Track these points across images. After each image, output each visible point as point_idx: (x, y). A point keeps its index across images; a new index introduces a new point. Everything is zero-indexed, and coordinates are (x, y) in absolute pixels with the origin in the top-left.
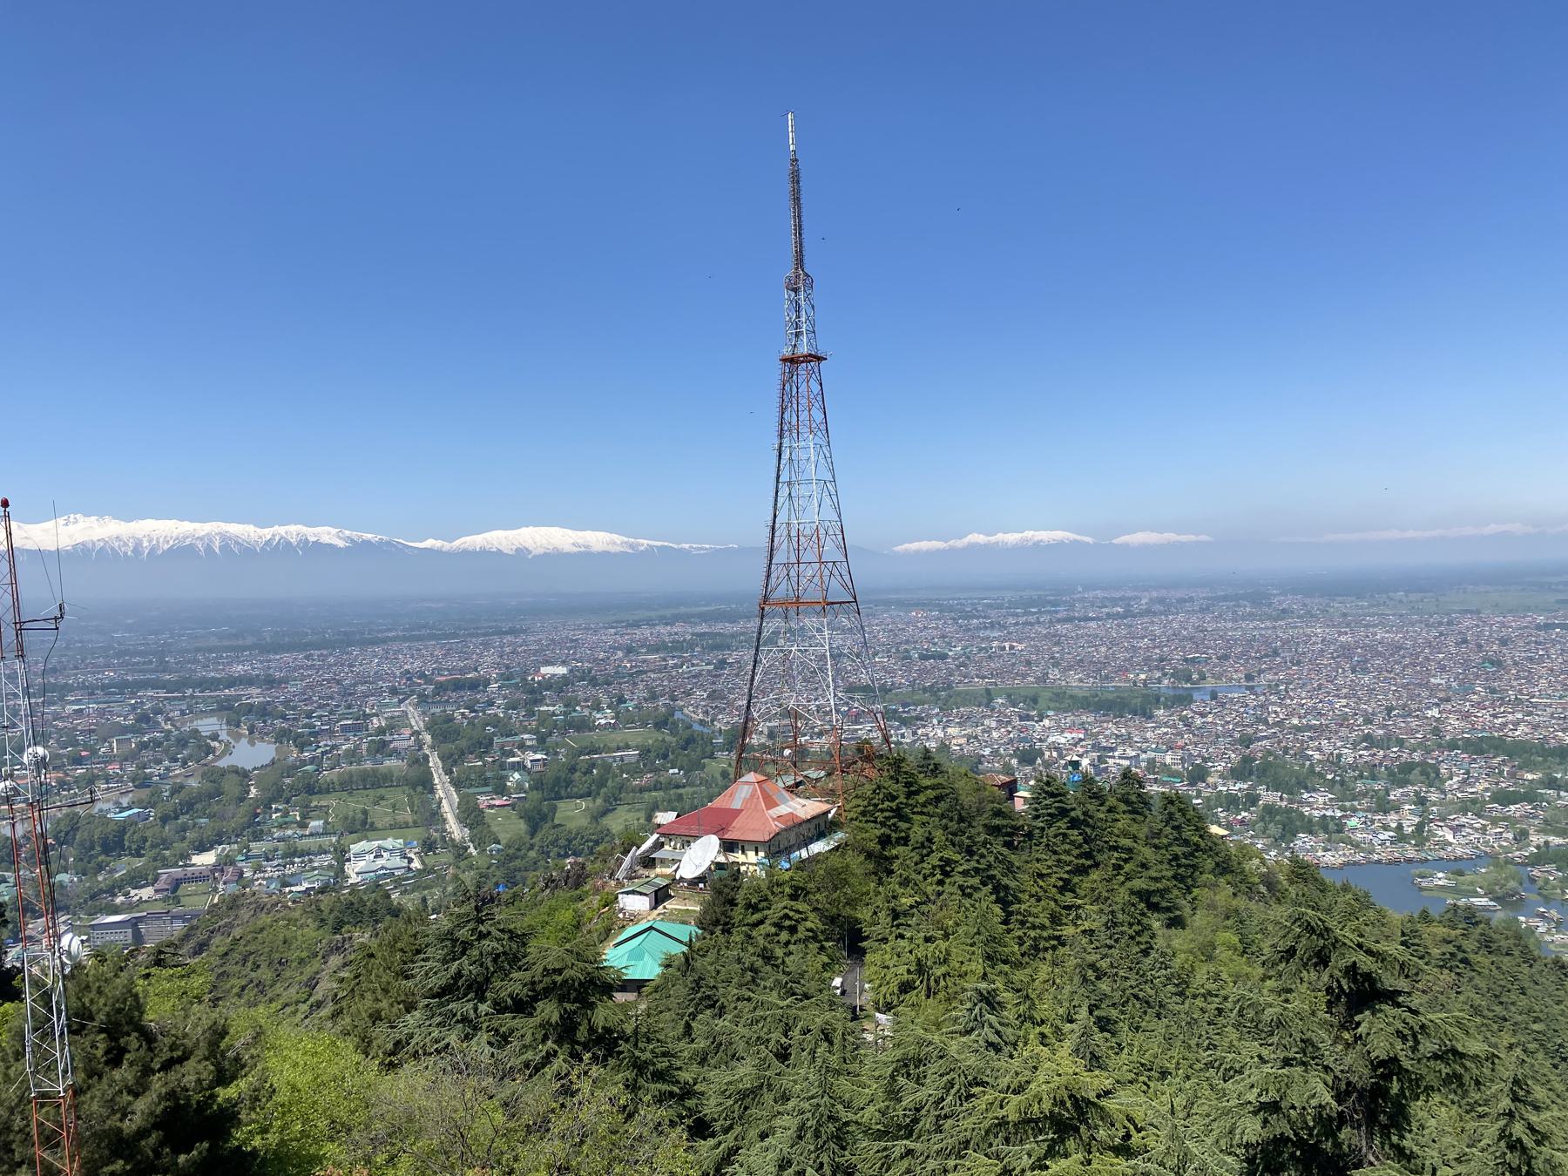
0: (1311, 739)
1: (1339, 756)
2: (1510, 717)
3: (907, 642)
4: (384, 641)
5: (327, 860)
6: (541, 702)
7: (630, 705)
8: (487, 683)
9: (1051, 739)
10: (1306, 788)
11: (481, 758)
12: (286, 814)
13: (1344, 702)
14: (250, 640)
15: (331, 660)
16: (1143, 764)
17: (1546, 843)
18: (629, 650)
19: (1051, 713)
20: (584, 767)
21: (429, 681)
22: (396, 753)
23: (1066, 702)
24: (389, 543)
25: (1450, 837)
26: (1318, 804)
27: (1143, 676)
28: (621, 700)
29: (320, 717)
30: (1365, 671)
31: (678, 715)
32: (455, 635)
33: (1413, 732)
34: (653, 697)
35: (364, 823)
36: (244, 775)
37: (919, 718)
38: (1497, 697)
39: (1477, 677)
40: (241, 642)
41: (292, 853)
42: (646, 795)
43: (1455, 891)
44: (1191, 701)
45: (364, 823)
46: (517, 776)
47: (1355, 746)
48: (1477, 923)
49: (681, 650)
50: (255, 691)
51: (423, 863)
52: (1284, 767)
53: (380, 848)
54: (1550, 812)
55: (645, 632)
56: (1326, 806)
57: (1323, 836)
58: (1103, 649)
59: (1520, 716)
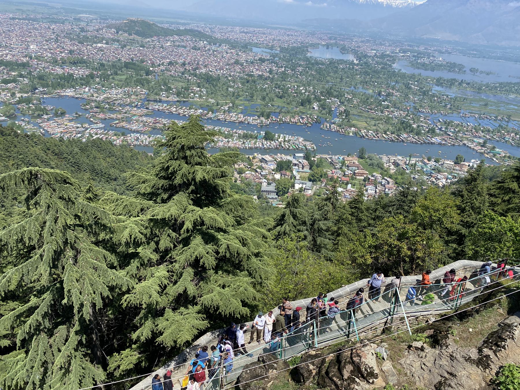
2: (4, 52)
17: (22, 96)
59: (8, 52)
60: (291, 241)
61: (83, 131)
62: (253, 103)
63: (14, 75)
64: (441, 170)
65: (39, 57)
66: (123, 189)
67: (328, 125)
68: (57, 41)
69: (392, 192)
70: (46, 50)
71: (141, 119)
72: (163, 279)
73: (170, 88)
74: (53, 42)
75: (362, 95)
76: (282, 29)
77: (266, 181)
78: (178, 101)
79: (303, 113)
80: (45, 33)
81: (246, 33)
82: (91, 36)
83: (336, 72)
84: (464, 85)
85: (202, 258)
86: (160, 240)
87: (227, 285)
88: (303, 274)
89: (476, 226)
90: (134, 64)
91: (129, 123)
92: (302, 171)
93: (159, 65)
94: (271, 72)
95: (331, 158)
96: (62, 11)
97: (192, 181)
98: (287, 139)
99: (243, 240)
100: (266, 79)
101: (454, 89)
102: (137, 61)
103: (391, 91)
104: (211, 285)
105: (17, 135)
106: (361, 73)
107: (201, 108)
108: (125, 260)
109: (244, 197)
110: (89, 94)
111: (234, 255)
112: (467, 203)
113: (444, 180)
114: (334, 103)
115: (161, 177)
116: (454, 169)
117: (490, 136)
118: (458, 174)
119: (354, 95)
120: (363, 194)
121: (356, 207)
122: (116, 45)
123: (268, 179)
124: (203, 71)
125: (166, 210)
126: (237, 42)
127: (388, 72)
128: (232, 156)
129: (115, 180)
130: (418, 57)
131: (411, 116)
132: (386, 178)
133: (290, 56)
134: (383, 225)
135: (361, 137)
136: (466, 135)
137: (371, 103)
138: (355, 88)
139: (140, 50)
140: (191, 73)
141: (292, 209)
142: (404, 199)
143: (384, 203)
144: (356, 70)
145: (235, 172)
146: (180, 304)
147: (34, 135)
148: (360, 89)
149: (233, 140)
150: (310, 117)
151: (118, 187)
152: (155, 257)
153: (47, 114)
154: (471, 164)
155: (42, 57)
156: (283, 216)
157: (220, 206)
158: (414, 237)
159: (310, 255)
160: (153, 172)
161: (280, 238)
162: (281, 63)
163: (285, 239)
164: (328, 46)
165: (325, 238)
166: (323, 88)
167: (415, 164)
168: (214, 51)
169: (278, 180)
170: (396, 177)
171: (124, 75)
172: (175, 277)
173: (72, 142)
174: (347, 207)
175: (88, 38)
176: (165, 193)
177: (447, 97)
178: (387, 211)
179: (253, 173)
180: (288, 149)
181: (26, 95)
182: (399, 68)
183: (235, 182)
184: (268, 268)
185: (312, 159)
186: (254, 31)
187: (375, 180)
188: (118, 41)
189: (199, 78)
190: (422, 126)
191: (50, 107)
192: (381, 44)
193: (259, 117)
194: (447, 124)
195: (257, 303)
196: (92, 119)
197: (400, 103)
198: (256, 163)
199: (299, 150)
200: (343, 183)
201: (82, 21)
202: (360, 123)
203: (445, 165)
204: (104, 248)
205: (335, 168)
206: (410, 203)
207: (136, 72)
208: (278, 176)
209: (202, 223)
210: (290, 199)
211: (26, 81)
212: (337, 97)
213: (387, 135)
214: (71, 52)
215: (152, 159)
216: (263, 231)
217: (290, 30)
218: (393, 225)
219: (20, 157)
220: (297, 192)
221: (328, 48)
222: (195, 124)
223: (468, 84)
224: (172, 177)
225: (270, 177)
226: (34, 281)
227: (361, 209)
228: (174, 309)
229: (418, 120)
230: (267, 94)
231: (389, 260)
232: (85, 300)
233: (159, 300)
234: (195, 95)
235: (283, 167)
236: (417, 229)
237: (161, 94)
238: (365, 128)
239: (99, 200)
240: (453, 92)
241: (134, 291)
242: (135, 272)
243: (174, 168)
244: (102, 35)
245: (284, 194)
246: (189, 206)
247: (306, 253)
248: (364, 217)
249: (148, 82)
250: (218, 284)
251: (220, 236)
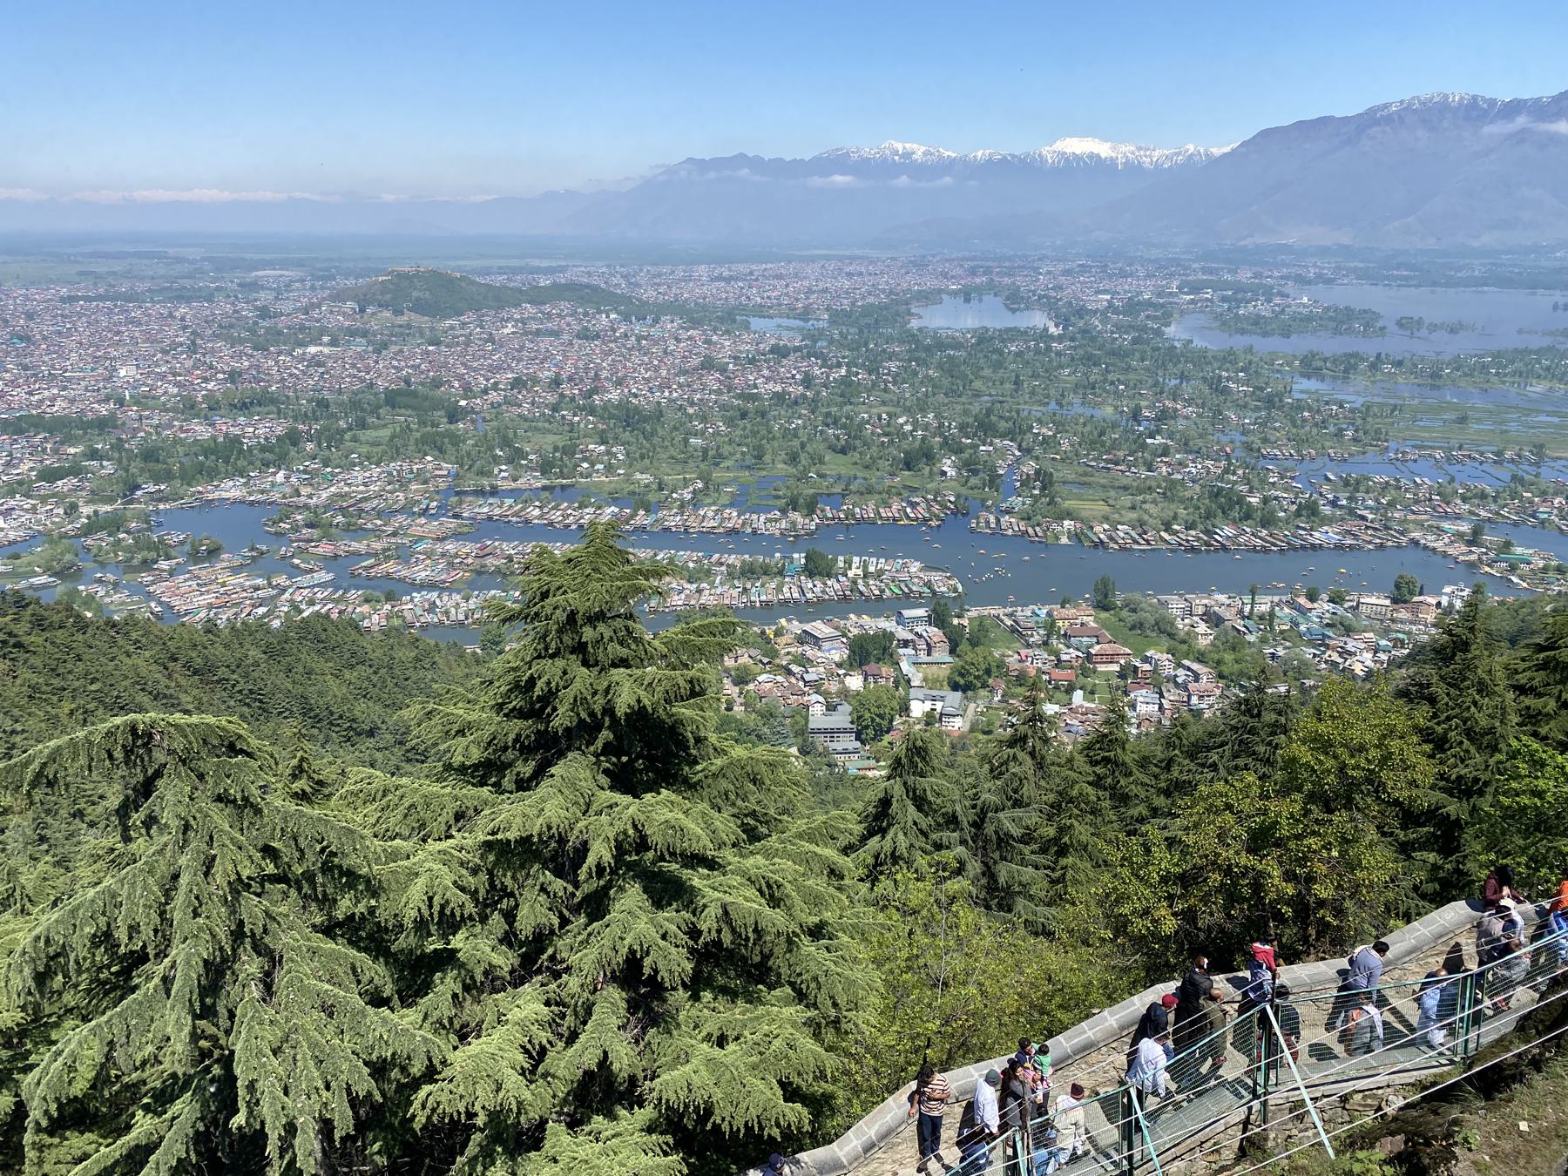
2: (46, 393)
39: (8, 353)
48: (27, 605)
60: (917, 880)
61: (273, 597)
62: (764, 473)
63: (74, 455)
64: (1354, 624)
66: (394, 760)
67: (992, 519)
68: (193, 349)
69: (1211, 706)
70: (163, 377)
71: (439, 548)
72: (534, 1028)
73: (521, 454)
74: (182, 353)
75: (1085, 425)
76: (828, 258)
77: (821, 699)
78: (544, 488)
79: (914, 490)
80: (161, 331)
81: (728, 280)
82: (289, 328)
83: (998, 365)
84: (1387, 368)
85: (648, 954)
86: (517, 905)
87: (731, 1034)
88: (964, 983)
89: (1490, 790)
90: (414, 394)
91: (407, 562)
92: (929, 659)
93: (485, 392)
94: (808, 381)
95: (1010, 615)
96: (207, 266)
97: (603, 715)
98: (872, 569)
99: (769, 886)
100: (796, 403)
101: (1360, 381)
102: (422, 384)
103: (1169, 404)
104: (683, 1039)
105: (82, 626)
106: (1073, 359)
107: (615, 501)
108: (415, 976)
109: (761, 751)
110: (288, 490)
111: (747, 939)
112: (1449, 719)
113: (1370, 655)
114: (1002, 453)
115: (511, 711)
116: (1393, 620)
117: (1490, 511)
118: (1409, 633)
119: (1060, 426)
120: (1122, 717)
121: (1106, 760)
122: (359, 345)
123: (826, 694)
124: (614, 395)
125: (533, 812)
126: (704, 308)
127: (1154, 349)
128: (713, 635)
129: (371, 733)
130: (1236, 300)
131: (1240, 472)
132: (1186, 662)
133: (861, 331)
134: (1199, 809)
135: (1096, 546)
136: (1414, 513)
137: (1115, 445)
138: (1061, 406)
139: (427, 353)
140: (578, 407)
141: (911, 779)
142: (1252, 722)
143: (1192, 739)
144: (1059, 354)
145: (725, 681)
146: (589, 1106)
147: (131, 621)
148: (1077, 407)
149: (712, 585)
150: (935, 500)
151: (379, 755)
152: (505, 960)
153: (168, 558)
154: (1445, 601)
155: (154, 398)
156: (885, 802)
157: (693, 787)
158: (1298, 837)
159: (983, 921)
160: (488, 698)
161: (882, 873)
162: (833, 354)
163: (899, 877)
164: (966, 295)
165: (1023, 863)
166: (966, 412)
167: (1272, 614)
168: (639, 338)
169: (858, 693)
170: (1216, 657)
171: (385, 426)
172: (570, 1020)
173: (241, 632)
174: (1080, 760)
175: (280, 333)
176: (526, 760)
177: (1341, 407)
178: (1203, 765)
179: (779, 678)
180: (879, 598)
181: (108, 508)
182: (1185, 336)
183: (729, 709)
184: (853, 970)
185: (956, 621)
186: (751, 273)
187: (1155, 671)
188: (365, 334)
189: (602, 418)
190: (1276, 498)
191: (175, 538)
192: (1123, 274)
193: (784, 511)
194: (1352, 486)
195: (829, 1088)
196: (296, 561)
197: (1201, 436)
198: (786, 648)
199: (909, 599)
200: (1057, 688)
201: (263, 287)
202: (1087, 505)
203: (1363, 608)
204: (350, 942)
205: (1028, 646)
206: (1273, 734)
207: (421, 417)
208: (855, 682)
209: (643, 844)
210: (900, 749)
211: (109, 467)
212: (1010, 435)
213: (1175, 533)
214: (233, 376)
215: (478, 662)
216: (830, 853)
217: (853, 259)
218: (1229, 807)
219: (94, 687)
220: (918, 727)
221: (967, 300)
222: (604, 549)
223: (1399, 364)
224: (542, 709)
225: (833, 687)
226: (144, 1063)
227: (1124, 764)
228: (574, 1124)
229: (1263, 481)
230: (803, 446)
231: (1229, 915)
232: (301, 1112)
233: (527, 1095)
234: (593, 465)
235: (868, 654)
236: (1307, 813)
237: (496, 471)
238: (1106, 519)
239: (328, 797)
240: (1356, 393)
241: (447, 1073)
242: (447, 1013)
243: (549, 683)
244: (318, 321)
245: (877, 737)
246: (600, 793)
247: (968, 916)
248: (1135, 789)
249: (456, 440)
250: (704, 1033)
251: (697, 879)
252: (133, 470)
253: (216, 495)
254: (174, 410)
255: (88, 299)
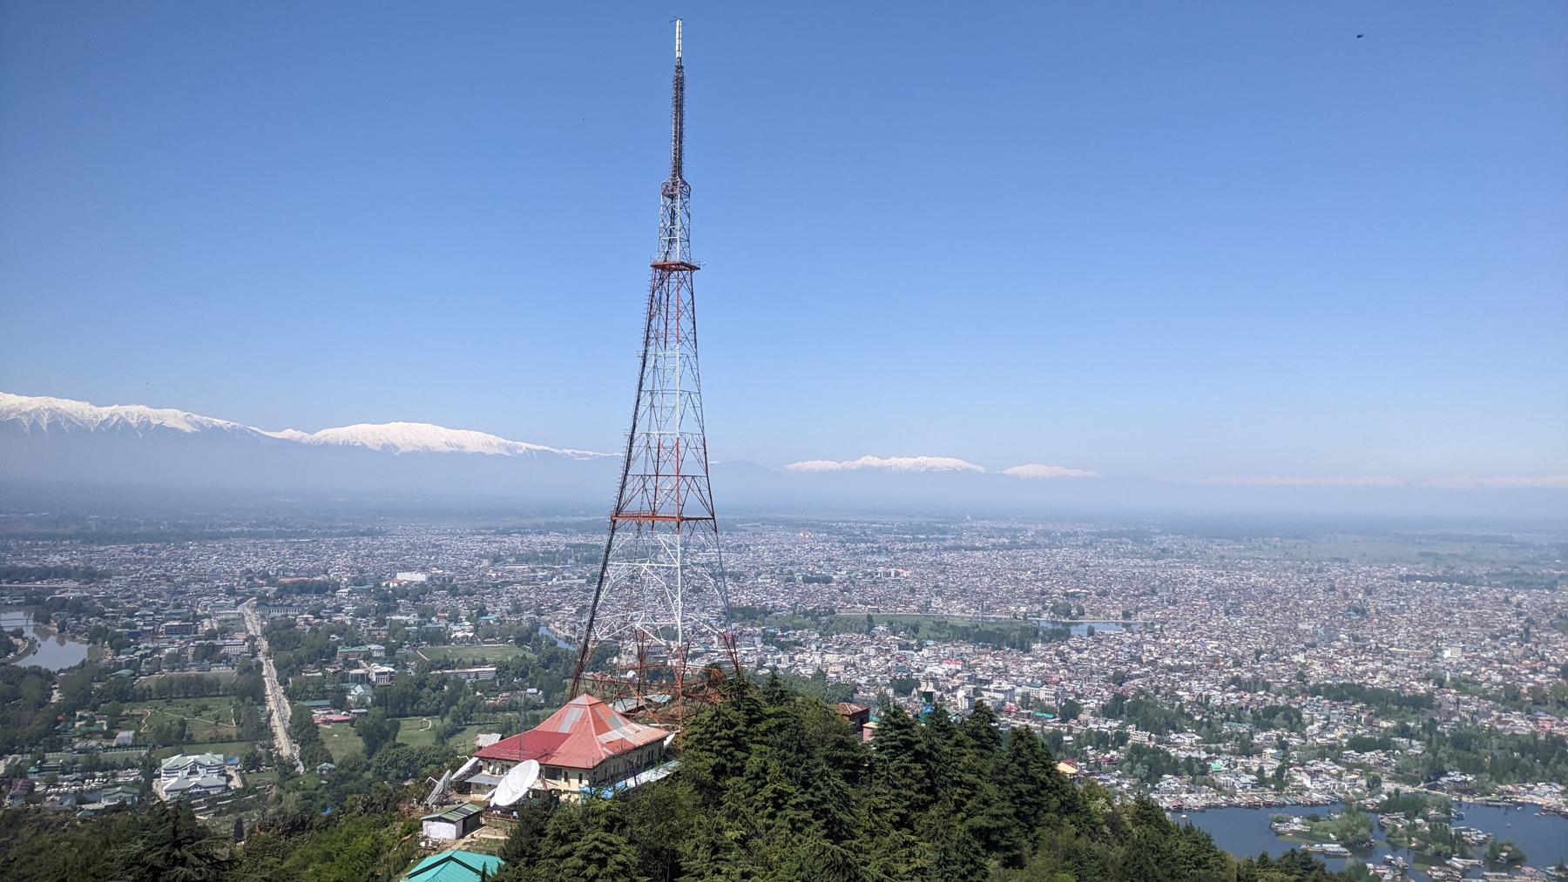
0: (1182, 679)
1: (1208, 697)
2: (1371, 665)
3: (792, 563)
4: (227, 536)
5: (133, 775)
6: (394, 610)
7: (491, 618)
8: (336, 587)
9: (928, 670)
10: (1174, 729)
11: (321, 668)
12: (91, 722)
13: (1215, 644)
14: (72, 529)
15: (164, 554)
16: (1018, 699)
18: (496, 559)
19: (930, 643)
20: (434, 682)
21: (272, 583)
22: (226, 659)
23: (947, 632)
24: (241, 430)
25: (1307, 782)
26: (1185, 744)
27: (1023, 609)
28: (482, 612)
29: (143, 616)
30: (1238, 613)
31: (543, 631)
32: (305, 534)
33: (1279, 676)
34: (518, 610)
35: (181, 735)
36: (46, 677)
37: (796, 643)
38: (1359, 645)
39: (1342, 624)
40: (61, 530)
41: (93, 766)
42: (499, 716)
43: (1311, 837)
44: (1069, 636)
45: (181, 735)
46: (359, 689)
47: (1224, 687)
49: (553, 561)
50: (70, 584)
51: (244, 781)
52: (1154, 707)
53: (196, 763)
54: (1402, 760)
55: (516, 541)
56: (1192, 747)
57: (1188, 778)
58: (987, 580)
59: (1379, 664)
63: (1387, 729)
65: (1466, 681)
68: (1525, 636)
70: (1488, 663)
153: (1463, 856)
155: (1475, 683)
181: (1408, 789)
191: (1476, 835)
211: (1417, 748)
252: (1441, 755)
253: (1528, 798)
254: (1495, 698)
255: (1425, 579)
